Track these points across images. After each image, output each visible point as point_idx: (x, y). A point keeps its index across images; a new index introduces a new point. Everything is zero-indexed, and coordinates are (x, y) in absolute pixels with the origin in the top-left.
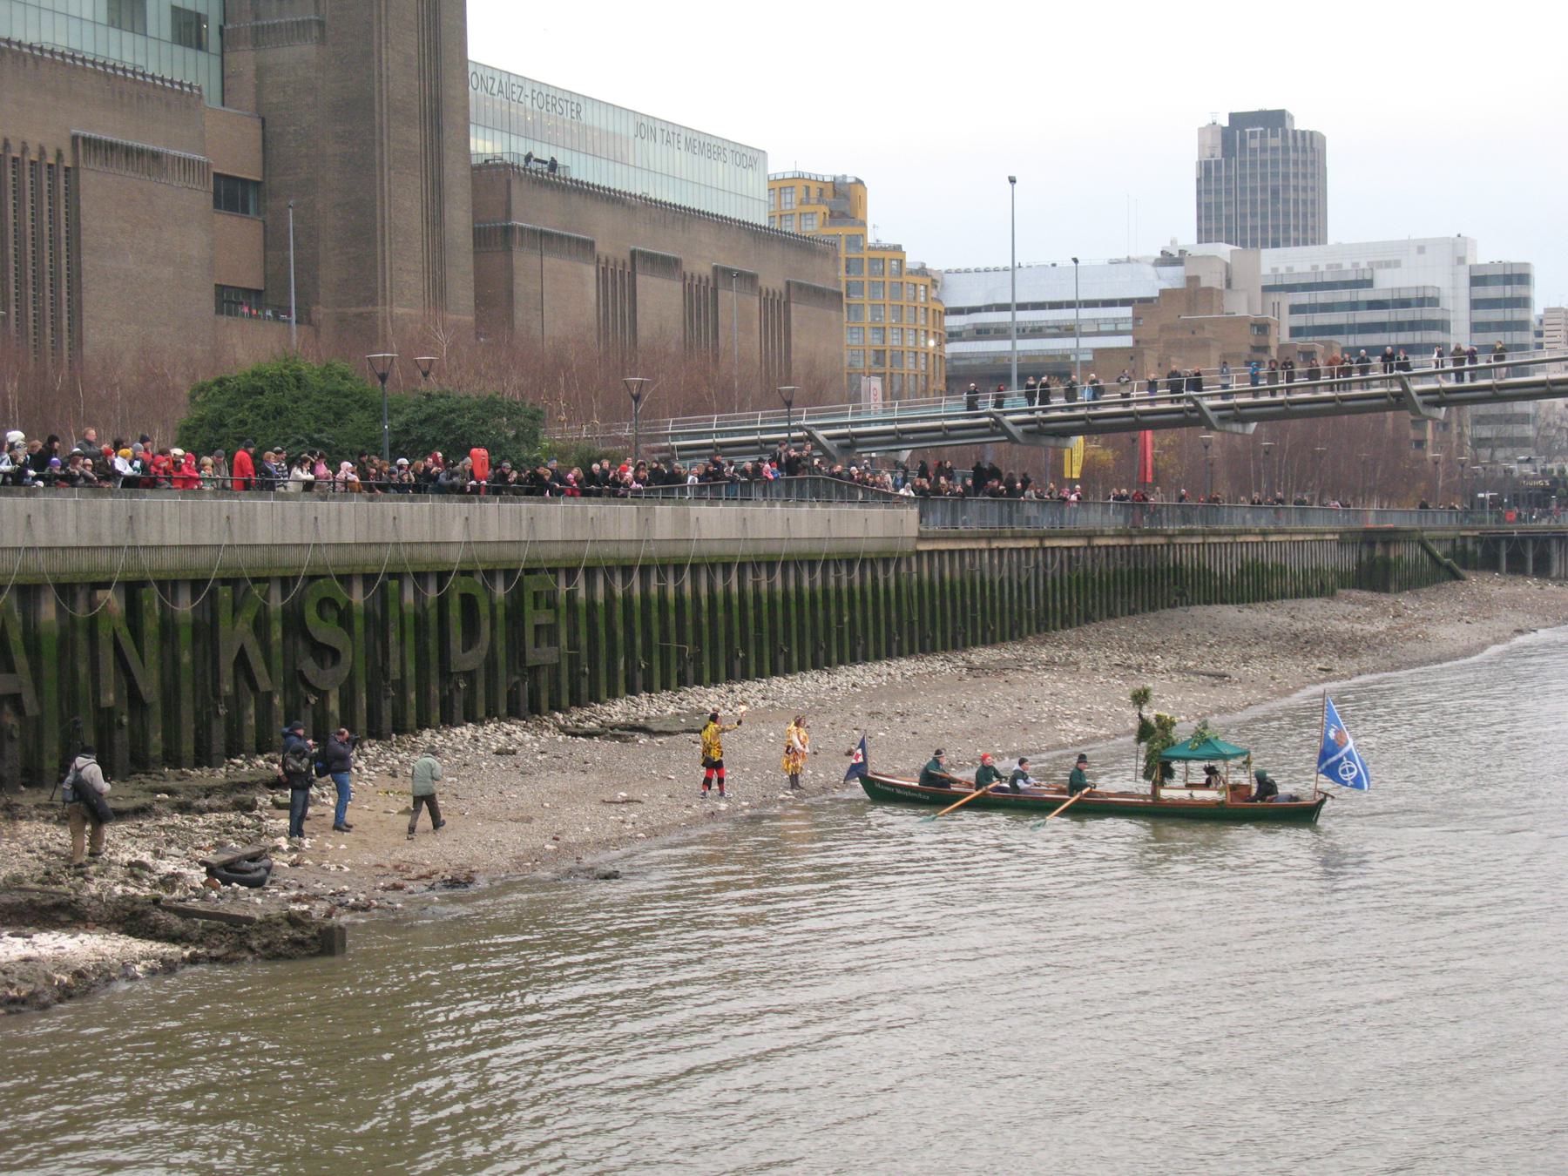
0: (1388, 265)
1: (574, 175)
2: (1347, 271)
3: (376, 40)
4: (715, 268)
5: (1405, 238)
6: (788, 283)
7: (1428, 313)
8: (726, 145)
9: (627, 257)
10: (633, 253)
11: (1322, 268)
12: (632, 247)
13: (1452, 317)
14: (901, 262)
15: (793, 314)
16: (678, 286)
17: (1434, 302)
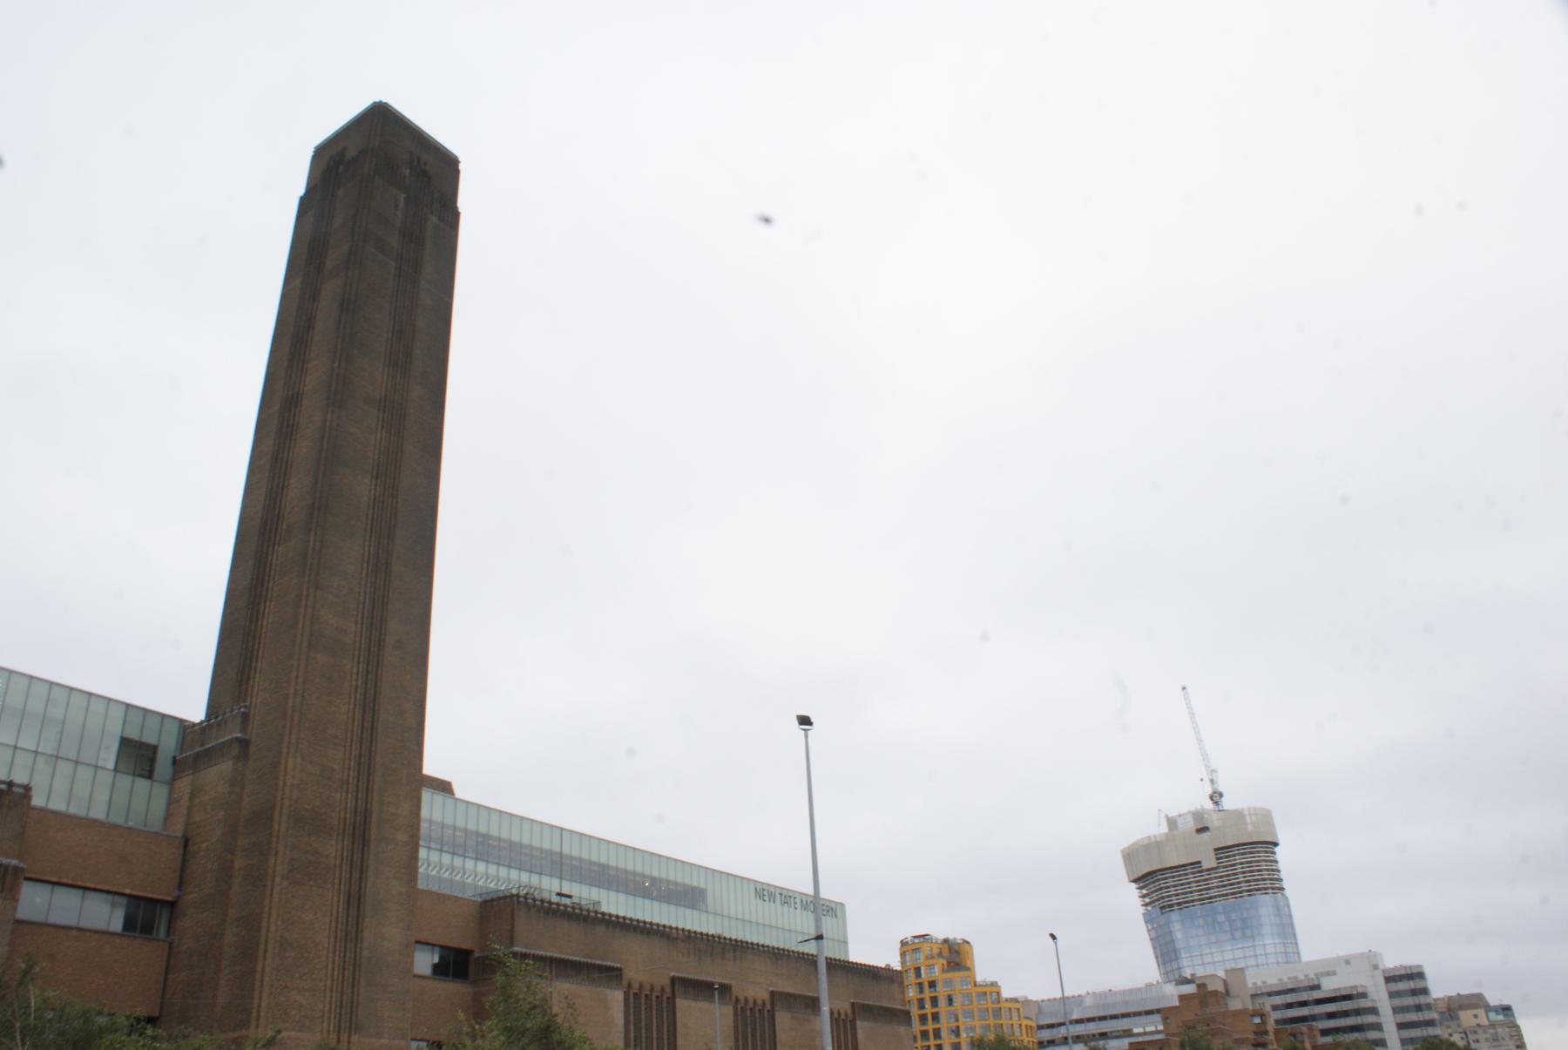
0: (1328, 974)
1: (604, 908)
2: (1302, 981)
3: (285, 750)
4: (772, 993)
5: (1334, 956)
6: (853, 1004)
7: (1363, 1003)
8: (797, 895)
9: (666, 983)
10: (673, 979)
11: (1285, 979)
12: (672, 974)
13: (1378, 1005)
14: (998, 993)
15: (859, 1031)
16: (728, 1009)
17: (1364, 995)
